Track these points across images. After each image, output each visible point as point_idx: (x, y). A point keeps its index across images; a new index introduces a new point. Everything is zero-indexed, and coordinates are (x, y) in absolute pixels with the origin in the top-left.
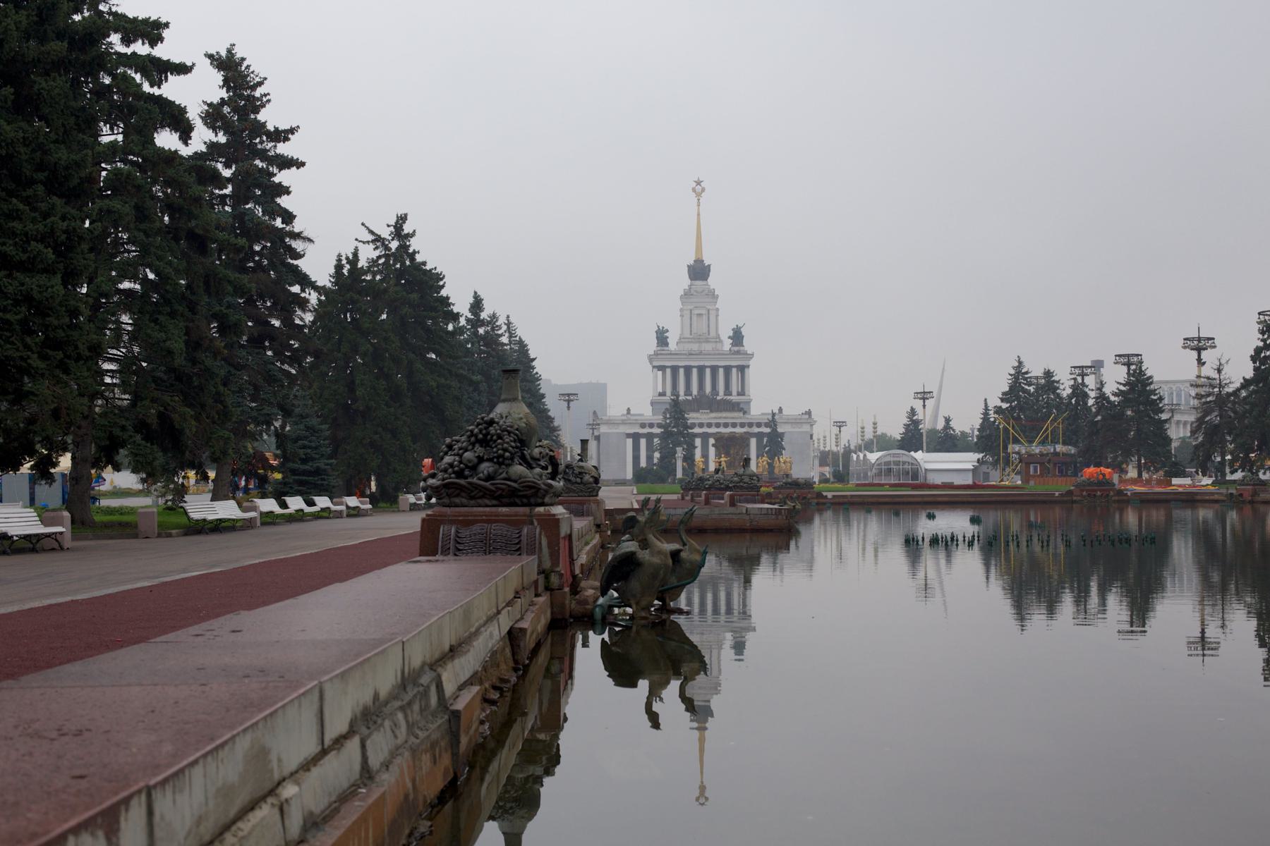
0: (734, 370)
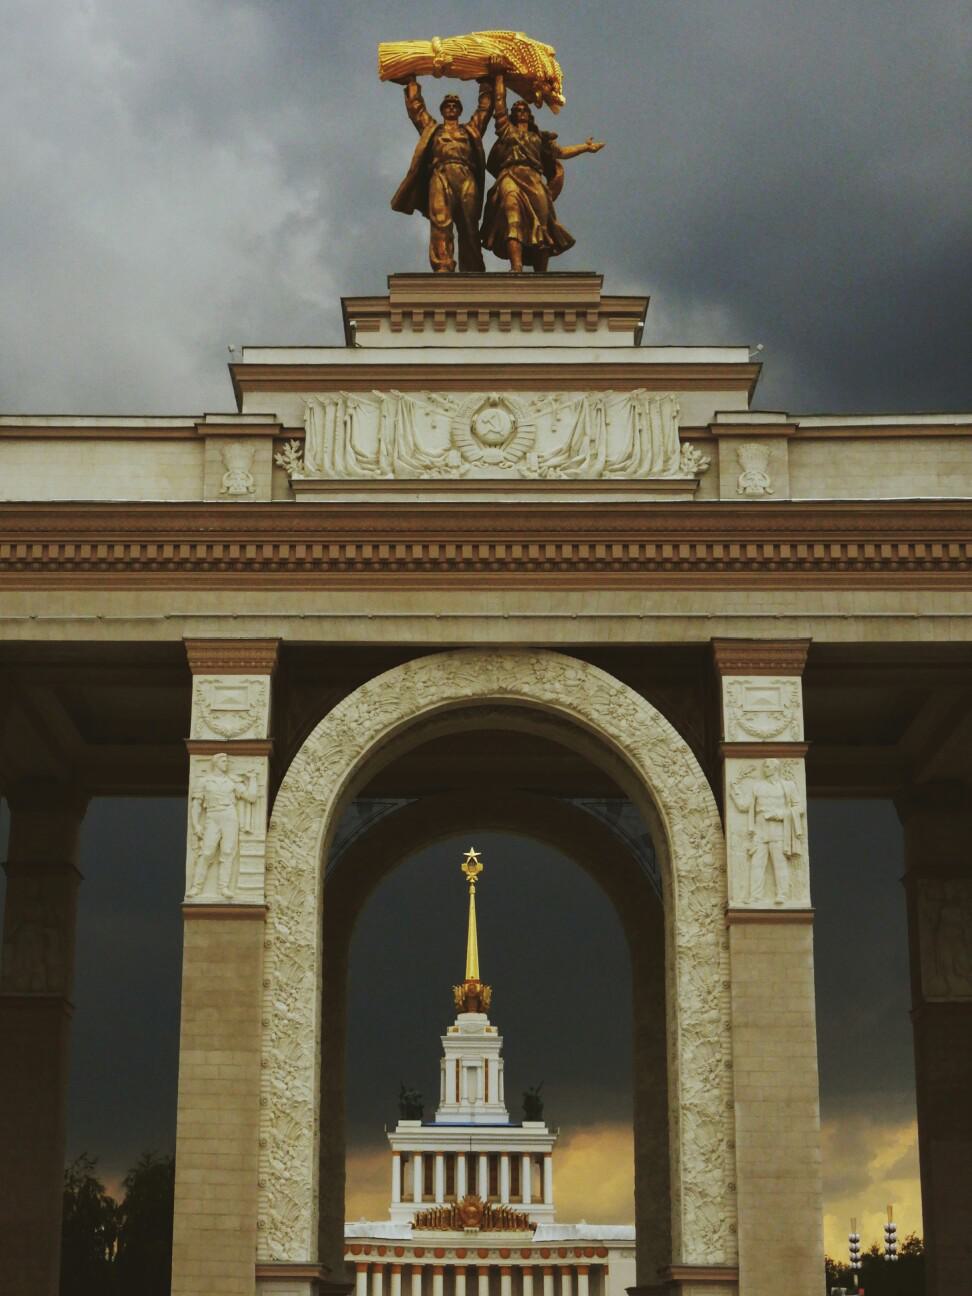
0: (526, 1161)
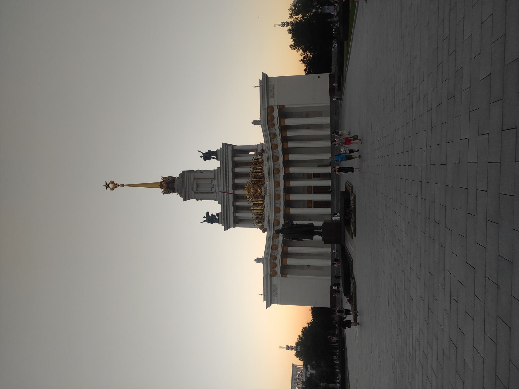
0: (236, 159)
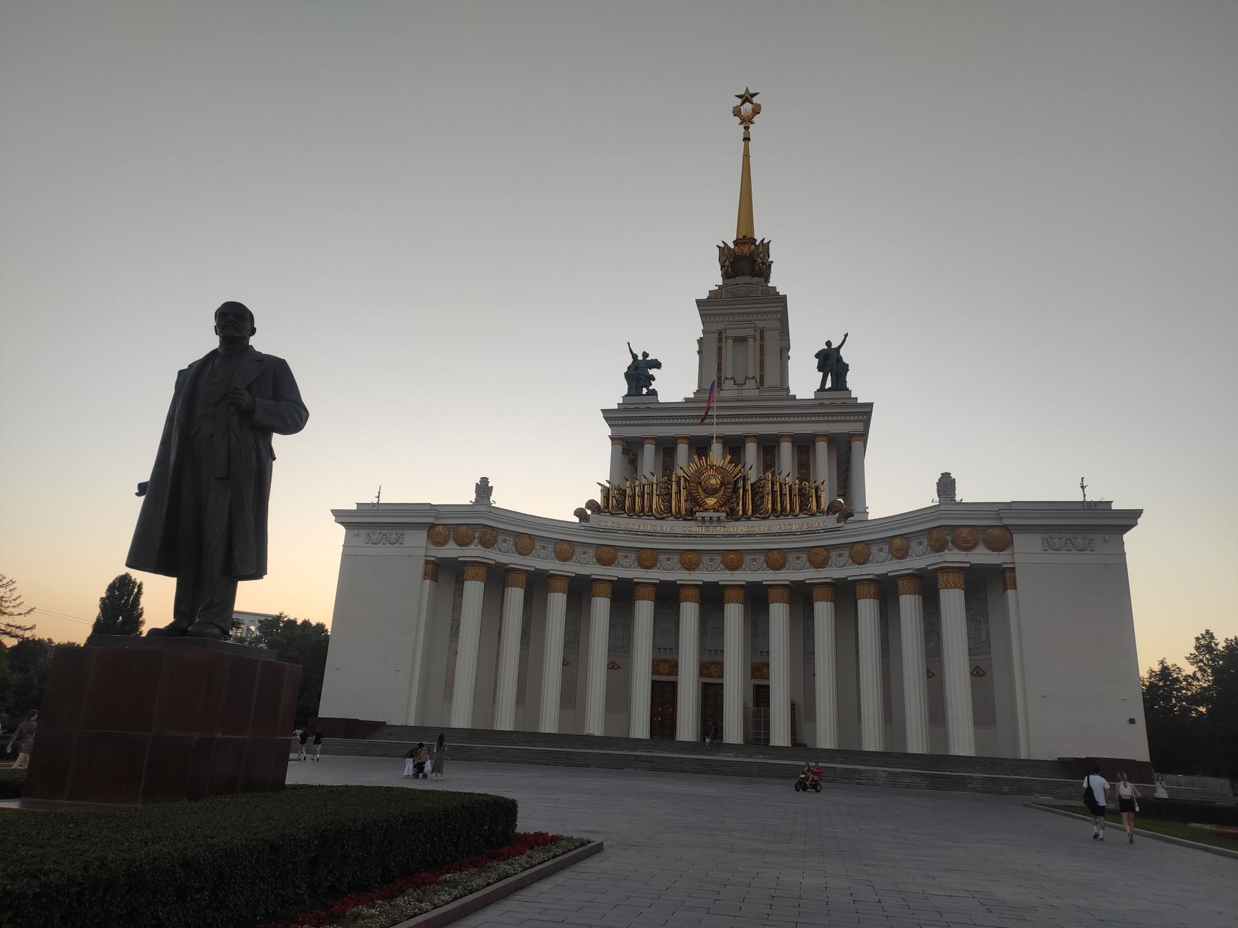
0: (822, 447)
